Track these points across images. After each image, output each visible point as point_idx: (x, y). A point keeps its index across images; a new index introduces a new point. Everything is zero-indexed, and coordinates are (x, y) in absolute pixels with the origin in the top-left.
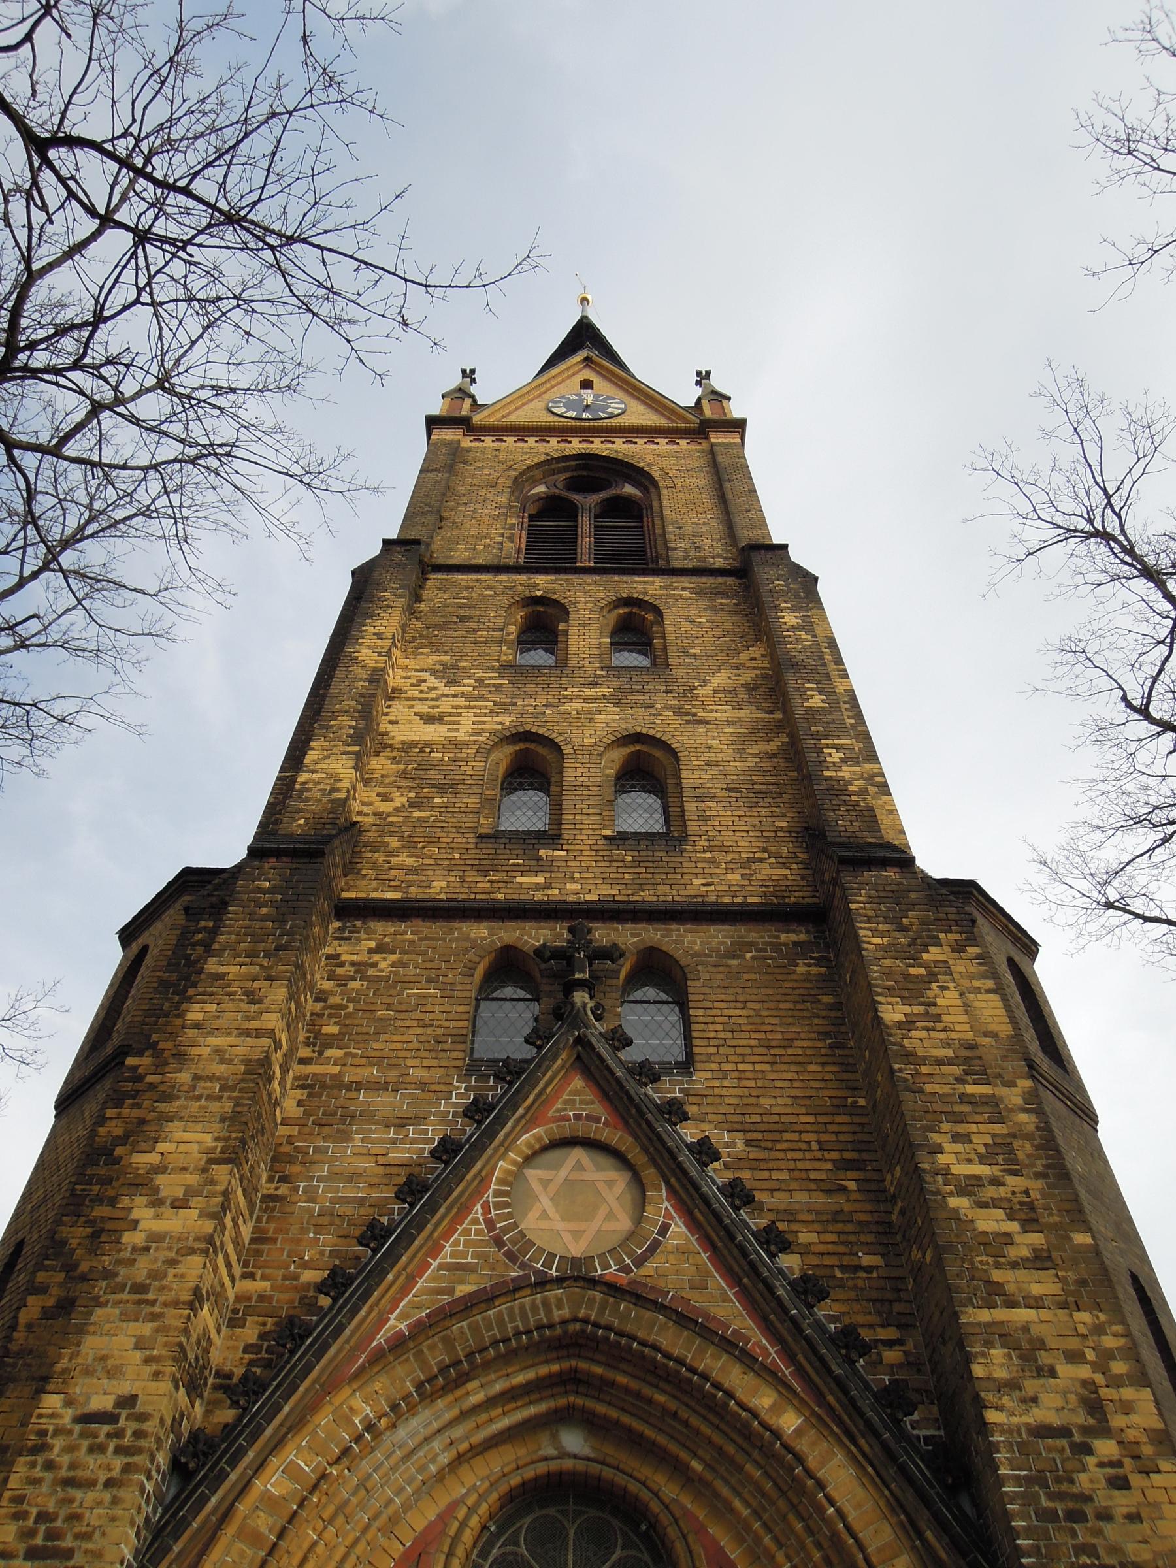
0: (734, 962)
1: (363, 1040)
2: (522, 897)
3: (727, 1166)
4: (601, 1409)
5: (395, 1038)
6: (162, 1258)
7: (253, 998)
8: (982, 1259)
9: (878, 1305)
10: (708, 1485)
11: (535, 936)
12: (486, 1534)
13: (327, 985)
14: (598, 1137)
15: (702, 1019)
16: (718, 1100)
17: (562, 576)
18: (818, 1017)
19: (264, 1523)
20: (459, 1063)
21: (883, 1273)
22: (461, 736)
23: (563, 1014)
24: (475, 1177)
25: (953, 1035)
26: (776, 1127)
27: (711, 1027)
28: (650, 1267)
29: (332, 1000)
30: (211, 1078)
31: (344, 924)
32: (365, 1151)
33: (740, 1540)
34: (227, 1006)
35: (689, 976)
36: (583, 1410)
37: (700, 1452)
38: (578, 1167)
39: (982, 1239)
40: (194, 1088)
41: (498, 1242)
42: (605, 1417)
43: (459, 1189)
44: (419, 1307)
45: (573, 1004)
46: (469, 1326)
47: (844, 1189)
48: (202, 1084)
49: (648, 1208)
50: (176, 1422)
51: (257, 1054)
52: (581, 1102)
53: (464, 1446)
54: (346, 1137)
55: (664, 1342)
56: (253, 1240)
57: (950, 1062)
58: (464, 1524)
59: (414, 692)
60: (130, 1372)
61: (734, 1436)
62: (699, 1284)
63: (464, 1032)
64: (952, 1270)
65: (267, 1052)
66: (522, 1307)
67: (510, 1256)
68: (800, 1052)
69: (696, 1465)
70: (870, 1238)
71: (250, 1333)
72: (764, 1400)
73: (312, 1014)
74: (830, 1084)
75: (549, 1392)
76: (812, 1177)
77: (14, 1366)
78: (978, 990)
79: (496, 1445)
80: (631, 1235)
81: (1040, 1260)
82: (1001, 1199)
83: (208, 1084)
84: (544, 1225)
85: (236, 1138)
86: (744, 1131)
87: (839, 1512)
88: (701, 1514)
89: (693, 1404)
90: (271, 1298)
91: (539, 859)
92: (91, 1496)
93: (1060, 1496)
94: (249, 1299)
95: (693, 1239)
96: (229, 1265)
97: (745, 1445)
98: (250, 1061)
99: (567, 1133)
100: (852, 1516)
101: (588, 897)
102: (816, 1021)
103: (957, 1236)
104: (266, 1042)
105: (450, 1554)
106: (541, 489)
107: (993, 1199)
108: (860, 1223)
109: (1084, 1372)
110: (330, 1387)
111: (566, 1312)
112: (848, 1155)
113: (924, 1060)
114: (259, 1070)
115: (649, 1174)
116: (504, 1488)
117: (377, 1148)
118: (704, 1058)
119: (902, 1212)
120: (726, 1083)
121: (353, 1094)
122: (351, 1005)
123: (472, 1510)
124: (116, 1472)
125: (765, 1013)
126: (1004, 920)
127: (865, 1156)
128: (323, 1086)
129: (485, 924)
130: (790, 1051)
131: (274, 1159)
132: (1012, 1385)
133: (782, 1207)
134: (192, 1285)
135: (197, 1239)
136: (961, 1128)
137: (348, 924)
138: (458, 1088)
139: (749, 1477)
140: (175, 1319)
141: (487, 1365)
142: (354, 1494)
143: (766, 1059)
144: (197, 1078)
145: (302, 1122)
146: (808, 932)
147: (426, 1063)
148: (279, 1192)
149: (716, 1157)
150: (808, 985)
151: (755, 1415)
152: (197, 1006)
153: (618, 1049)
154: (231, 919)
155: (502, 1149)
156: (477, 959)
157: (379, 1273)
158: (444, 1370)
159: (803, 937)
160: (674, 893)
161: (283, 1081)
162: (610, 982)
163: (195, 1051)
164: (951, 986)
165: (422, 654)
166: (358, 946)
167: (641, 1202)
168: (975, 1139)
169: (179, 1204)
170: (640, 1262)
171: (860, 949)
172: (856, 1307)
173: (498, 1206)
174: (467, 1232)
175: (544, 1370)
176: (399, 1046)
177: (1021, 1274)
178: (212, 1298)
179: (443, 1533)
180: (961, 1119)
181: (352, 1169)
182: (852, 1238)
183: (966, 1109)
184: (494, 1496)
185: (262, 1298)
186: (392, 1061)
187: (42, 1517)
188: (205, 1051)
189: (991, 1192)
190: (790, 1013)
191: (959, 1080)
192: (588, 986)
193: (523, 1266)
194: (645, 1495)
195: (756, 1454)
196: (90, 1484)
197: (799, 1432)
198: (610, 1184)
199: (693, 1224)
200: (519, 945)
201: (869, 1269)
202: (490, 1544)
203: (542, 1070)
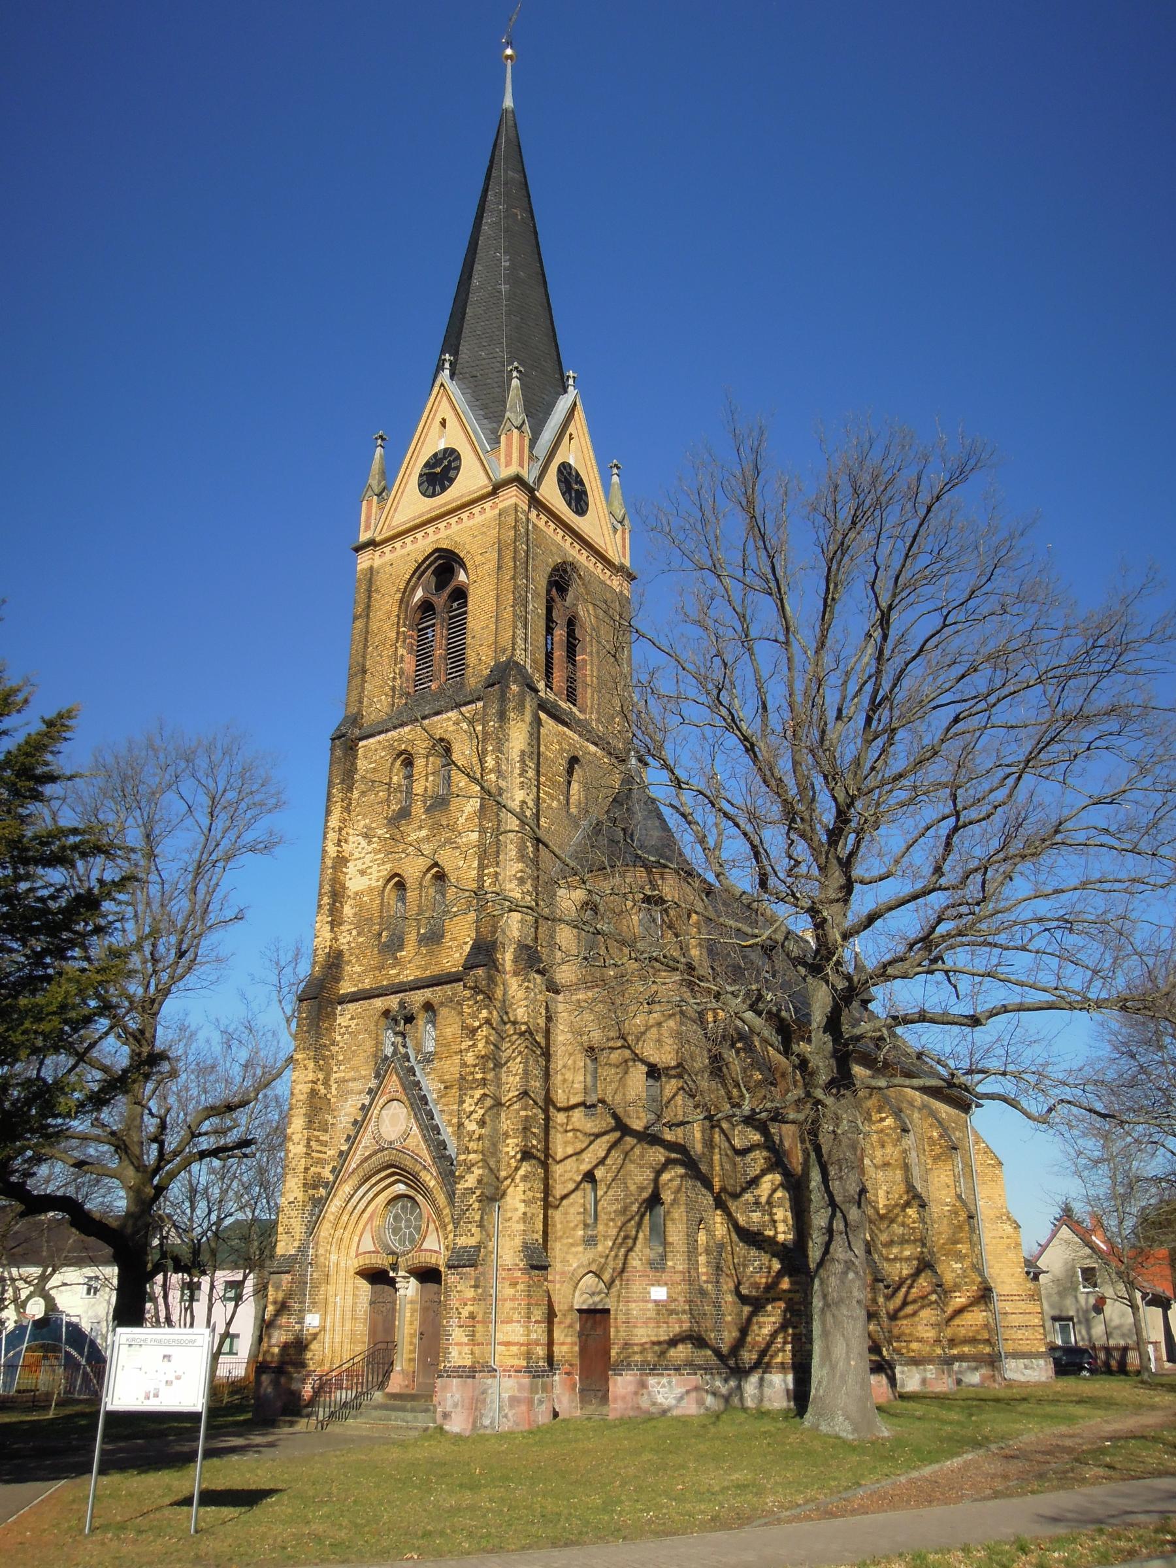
19: (332, 1218)
22: (374, 884)
59: (357, 855)
91: (396, 958)
106: (419, 594)
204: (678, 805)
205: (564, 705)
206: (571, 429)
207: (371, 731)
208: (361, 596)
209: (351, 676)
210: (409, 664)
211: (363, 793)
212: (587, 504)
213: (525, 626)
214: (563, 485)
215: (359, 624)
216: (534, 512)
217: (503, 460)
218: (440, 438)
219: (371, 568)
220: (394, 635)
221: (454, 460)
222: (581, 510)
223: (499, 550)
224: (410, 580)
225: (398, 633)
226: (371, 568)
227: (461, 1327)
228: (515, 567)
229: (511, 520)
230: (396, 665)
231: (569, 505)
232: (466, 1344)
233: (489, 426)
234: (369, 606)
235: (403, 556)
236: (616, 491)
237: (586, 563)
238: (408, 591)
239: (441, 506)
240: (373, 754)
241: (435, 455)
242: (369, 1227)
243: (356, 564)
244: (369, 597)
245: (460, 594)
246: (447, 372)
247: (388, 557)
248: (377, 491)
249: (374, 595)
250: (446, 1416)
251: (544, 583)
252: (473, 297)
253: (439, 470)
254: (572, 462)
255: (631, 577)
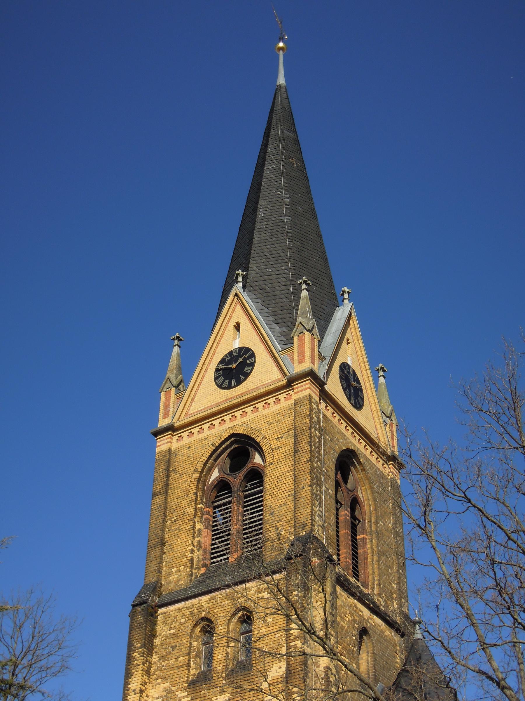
17: (213, 595)
106: (215, 474)
165: (158, 684)
204: (491, 673)
205: (353, 580)
206: (348, 335)
207: (172, 598)
208: (160, 475)
209: (150, 548)
210: (206, 538)
211: (163, 658)
212: (363, 400)
213: (320, 504)
214: (344, 382)
215: (159, 500)
216: (324, 404)
217: (296, 357)
218: (235, 339)
219: (170, 450)
220: (191, 511)
221: (249, 358)
222: (359, 406)
223: (295, 436)
224: (207, 461)
225: (196, 509)
226: (170, 450)
228: (311, 450)
229: (305, 410)
230: (194, 538)
231: (349, 399)
233: (279, 330)
234: (167, 485)
235: (200, 440)
236: (383, 389)
237: (364, 451)
238: (206, 471)
239: (237, 397)
240: (173, 620)
241: (231, 353)
243: (156, 447)
244: (168, 476)
245: (256, 476)
246: (240, 285)
247: (186, 440)
248: (175, 383)
249: (172, 475)
251: (333, 466)
252: (259, 226)
253: (234, 366)
254: (350, 363)
255: (400, 466)
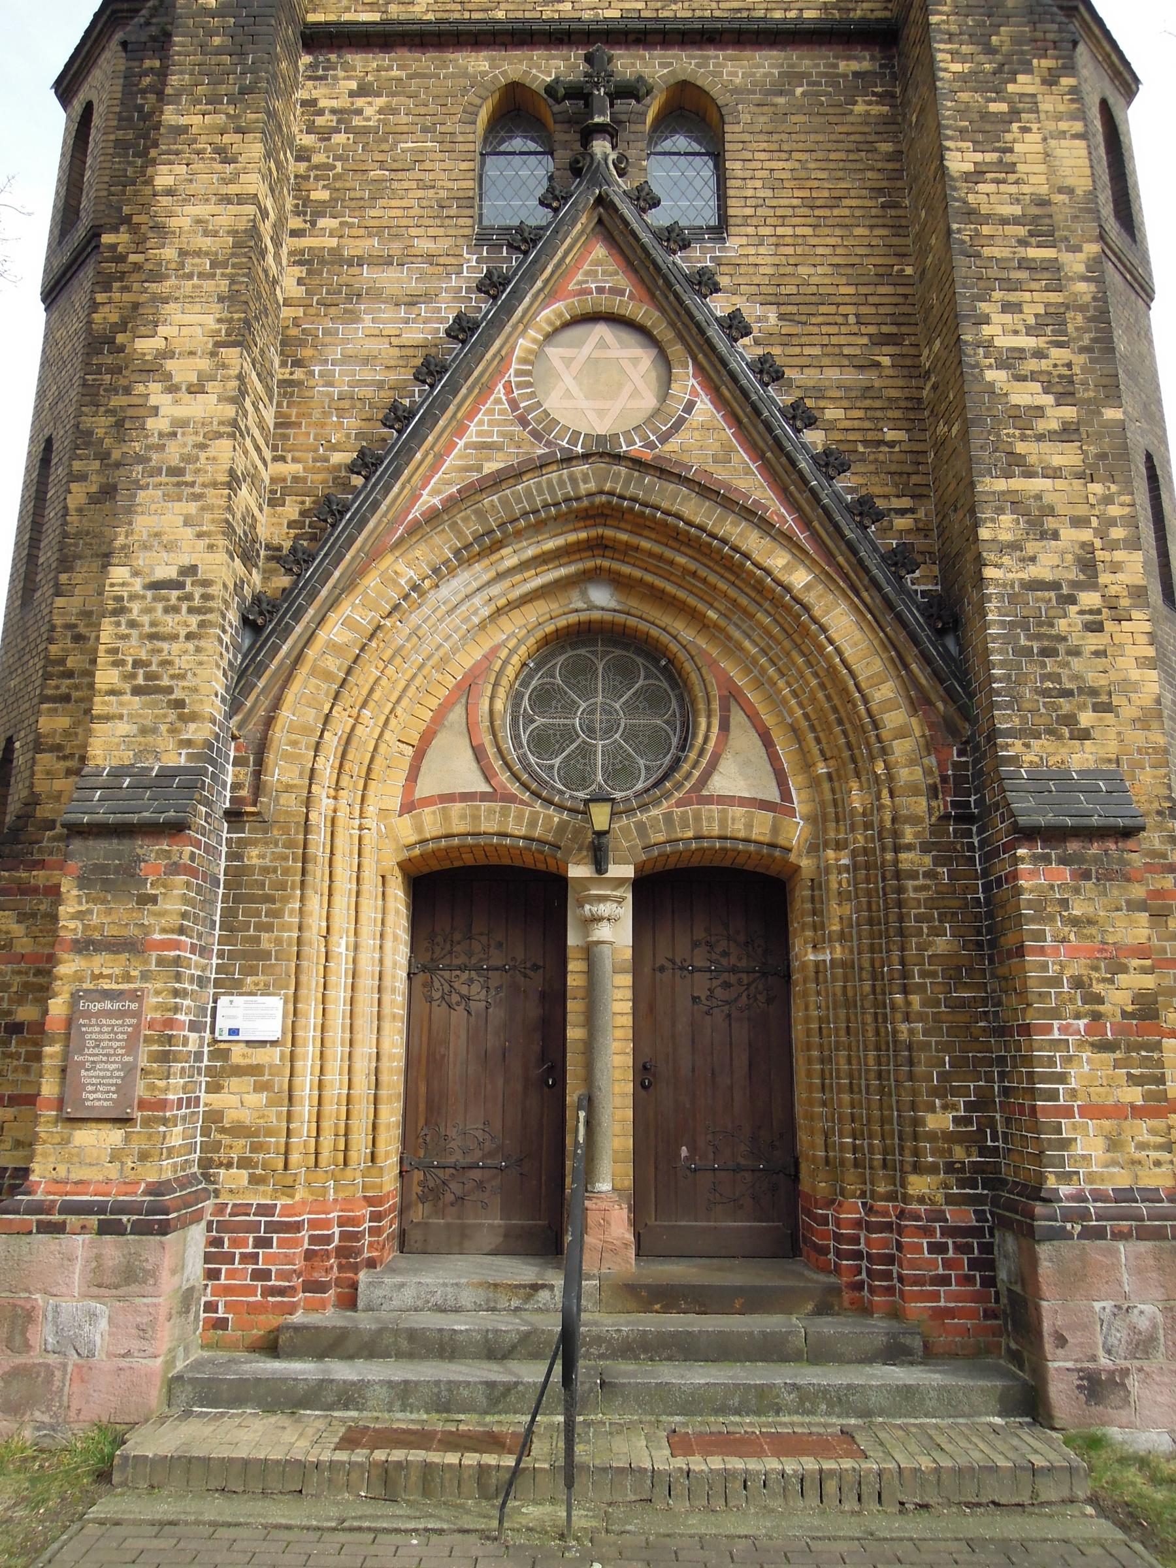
0: (781, 100)
1: (360, 207)
2: (528, 15)
3: (757, 342)
4: (626, 569)
5: (393, 203)
6: (190, 443)
7: (225, 156)
8: (1009, 431)
9: (896, 478)
10: (722, 630)
11: (546, 68)
12: (526, 670)
13: (308, 140)
14: (622, 312)
15: (739, 174)
16: (751, 270)
18: (872, 169)
19: (333, 664)
20: (467, 231)
21: (905, 447)
23: (581, 169)
24: (495, 356)
25: (1026, 189)
26: (814, 299)
27: (750, 183)
28: (674, 444)
29: (318, 159)
30: (198, 253)
31: (316, 59)
32: (377, 332)
33: (747, 671)
34: (198, 166)
35: (727, 119)
36: (610, 570)
37: (716, 604)
38: (602, 344)
39: (1012, 413)
40: (182, 265)
41: (523, 421)
42: (630, 577)
43: (480, 368)
44: (449, 483)
45: (592, 156)
46: (499, 499)
47: (878, 365)
48: (189, 261)
49: (673, 385)
50: (239, 587)
51: (243, 224)
52: (604, 273)
53: (502, 602)
54: (353, 317)
55: (686, 512)
56: (277, 426)
57: (1016, 221)
58: (506, 662)
60: (185, 546)
61: (747, 590)
62: (723, 459)
63: (471, 194)
64: (976, 443)
65: (254, 221)
66: (549, 482)
67: (536, 434)
68: (847, 212)
69: (712, 614)
70: (898, 414)
71: (291, 510)
72: (778, 560)
73: (296, 177)
74: (876, 251)
75: (577, 556)
76: (846, 352)
77: (76, 545)
78: (1062, 134)
79: (531, 601)
80: (657, 412)
81: (1067, 433)
82: (1041, 372)
83: (197, 260)
84: (568, 404)
85: (239, 319)
86: (778, 304)
87: (838, 650)
88: (714, 653)
89: (711, 564)
90: (305, 479)
92: (176, 647)
93: (1039, 637)
94: (284, 480)
95: (719, 416)
96: (258, 449)
97: (758, 598)
98: (237, 232)
99: (589, 309)
100: (848, 653)
101: (609, 14)
102: (869, 174)
103: (988, 409)
104: (251, 209)
105: (496, 685)
107: (1032, 372)
108: (889, 399)
109: (1086, 535)
110: (374, 555)
111: (592, 486)
112: (885, 329)
113: (987, 219)
114: (248, 242)
115: (676, 350)
116: (539, 634)
117: (390, 329)
118: (739, 221)
119: (935, 387)
120: (762, 250)
121: (355, 270)
122: (339, 164)
123: (512, 652)
124: (194, 628)
125: (812, 165)
126: (1108, 48)
127: (904, 330)
128: (323, 262)
129: (484, 54)
130: (836, 212)
131: (284, 343)
132: (1015, 546)
133: (811, 384)
134: (228, 467)
135: (221, 423)
136: (1013, 297)
137: (321, 58)
138: (468, 261)
139: (760, 624)
140: (216, 498)
141: (518, 534)
142: (408, 640)
143: (810, 221)
144: (183, 253)
145: (308, 302)
146: (872, 58)
147: (432, 232)
148: (295, 377)
149: (746, 331)
150: (866, 129)
151: (768, 573)
152: (163, 169)
153: (644, 210)
154: (179, 54)
155: (521, 327)
156: (478, 101)
157: (406, 452)
158: (478, 538)
159: (866, 65)
160: (714, 5)
161: (277, 256)
162: (634, 128)
163: (174, 223)
164: (1035, 127)
166: (338, 86)
167: (667, 380)
168: (1026, 309)
169: (196, 389)
170: (664, 438)
171: (934, 78)
172: (874, 479)
173: (519, 385)
174: (490, 412)
175: (572, 537)
176: (399, 213)
177: (1045, 447)
178: (249, 479)
179: (489, 668)
180: (1016, 286)
181: (369, 349)
182: (879, 414)
183: (1023, 275)
184: (532, 640)
185: (296, 479)
186: (394, 231)
187: (137, 663)
188: (186, 223)
189: (1032, 365)
190: (841, 164)
191: (1023, 243)
192: (610, 132)
193: (549, 444)
194: (665, 638)
195: (767, 605)
196: (175, 637)
197: (808, 587)
198: (635, 361)
199: (719, 400)
200: (527, 82)
201: (891, 444)
202: (530, 676)
203: (560, 236)
227: (1104, 1047)
232: (1137, 1112)
242: (457, 715)
250: (1096, 1387)
